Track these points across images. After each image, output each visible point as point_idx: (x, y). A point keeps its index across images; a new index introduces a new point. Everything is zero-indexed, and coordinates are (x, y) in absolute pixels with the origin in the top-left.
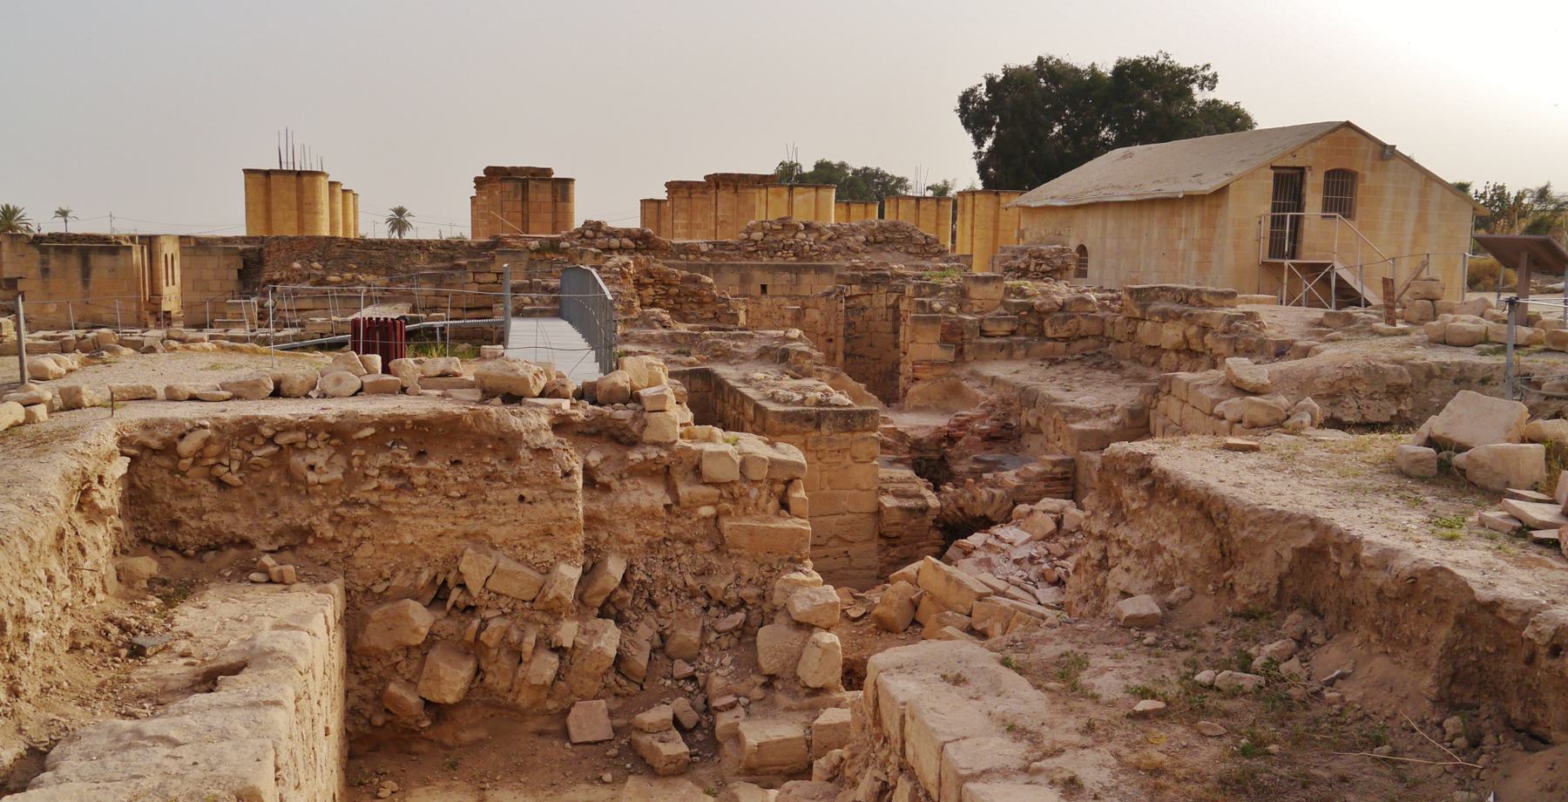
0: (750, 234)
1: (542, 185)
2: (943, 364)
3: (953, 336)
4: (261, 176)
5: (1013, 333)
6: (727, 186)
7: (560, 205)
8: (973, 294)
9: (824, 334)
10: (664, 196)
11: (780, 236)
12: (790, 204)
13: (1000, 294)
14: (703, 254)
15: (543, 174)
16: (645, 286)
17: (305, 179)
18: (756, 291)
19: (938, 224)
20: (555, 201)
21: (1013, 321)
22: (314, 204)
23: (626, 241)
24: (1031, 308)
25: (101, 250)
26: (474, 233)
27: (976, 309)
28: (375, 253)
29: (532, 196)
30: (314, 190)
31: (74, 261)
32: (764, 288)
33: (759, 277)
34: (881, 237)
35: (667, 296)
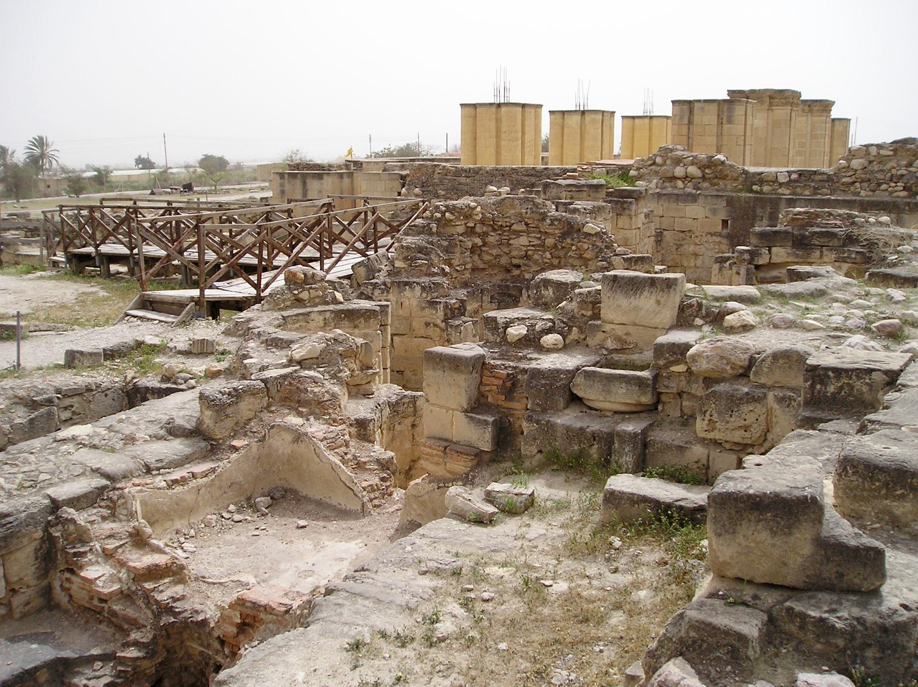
0: (849, 160)
4: (471, 110)
7: (726, 126)
8: (607, 312)
13: (669, 314)
14: (781, 185)
16: (518, 234)
17: (503, 109)
20: (720, 123)
22: (611, 127)
25: (315, 176)
28: (463, 180)
29: (697, 118)
30: (538, 118)
31: (298, 183)
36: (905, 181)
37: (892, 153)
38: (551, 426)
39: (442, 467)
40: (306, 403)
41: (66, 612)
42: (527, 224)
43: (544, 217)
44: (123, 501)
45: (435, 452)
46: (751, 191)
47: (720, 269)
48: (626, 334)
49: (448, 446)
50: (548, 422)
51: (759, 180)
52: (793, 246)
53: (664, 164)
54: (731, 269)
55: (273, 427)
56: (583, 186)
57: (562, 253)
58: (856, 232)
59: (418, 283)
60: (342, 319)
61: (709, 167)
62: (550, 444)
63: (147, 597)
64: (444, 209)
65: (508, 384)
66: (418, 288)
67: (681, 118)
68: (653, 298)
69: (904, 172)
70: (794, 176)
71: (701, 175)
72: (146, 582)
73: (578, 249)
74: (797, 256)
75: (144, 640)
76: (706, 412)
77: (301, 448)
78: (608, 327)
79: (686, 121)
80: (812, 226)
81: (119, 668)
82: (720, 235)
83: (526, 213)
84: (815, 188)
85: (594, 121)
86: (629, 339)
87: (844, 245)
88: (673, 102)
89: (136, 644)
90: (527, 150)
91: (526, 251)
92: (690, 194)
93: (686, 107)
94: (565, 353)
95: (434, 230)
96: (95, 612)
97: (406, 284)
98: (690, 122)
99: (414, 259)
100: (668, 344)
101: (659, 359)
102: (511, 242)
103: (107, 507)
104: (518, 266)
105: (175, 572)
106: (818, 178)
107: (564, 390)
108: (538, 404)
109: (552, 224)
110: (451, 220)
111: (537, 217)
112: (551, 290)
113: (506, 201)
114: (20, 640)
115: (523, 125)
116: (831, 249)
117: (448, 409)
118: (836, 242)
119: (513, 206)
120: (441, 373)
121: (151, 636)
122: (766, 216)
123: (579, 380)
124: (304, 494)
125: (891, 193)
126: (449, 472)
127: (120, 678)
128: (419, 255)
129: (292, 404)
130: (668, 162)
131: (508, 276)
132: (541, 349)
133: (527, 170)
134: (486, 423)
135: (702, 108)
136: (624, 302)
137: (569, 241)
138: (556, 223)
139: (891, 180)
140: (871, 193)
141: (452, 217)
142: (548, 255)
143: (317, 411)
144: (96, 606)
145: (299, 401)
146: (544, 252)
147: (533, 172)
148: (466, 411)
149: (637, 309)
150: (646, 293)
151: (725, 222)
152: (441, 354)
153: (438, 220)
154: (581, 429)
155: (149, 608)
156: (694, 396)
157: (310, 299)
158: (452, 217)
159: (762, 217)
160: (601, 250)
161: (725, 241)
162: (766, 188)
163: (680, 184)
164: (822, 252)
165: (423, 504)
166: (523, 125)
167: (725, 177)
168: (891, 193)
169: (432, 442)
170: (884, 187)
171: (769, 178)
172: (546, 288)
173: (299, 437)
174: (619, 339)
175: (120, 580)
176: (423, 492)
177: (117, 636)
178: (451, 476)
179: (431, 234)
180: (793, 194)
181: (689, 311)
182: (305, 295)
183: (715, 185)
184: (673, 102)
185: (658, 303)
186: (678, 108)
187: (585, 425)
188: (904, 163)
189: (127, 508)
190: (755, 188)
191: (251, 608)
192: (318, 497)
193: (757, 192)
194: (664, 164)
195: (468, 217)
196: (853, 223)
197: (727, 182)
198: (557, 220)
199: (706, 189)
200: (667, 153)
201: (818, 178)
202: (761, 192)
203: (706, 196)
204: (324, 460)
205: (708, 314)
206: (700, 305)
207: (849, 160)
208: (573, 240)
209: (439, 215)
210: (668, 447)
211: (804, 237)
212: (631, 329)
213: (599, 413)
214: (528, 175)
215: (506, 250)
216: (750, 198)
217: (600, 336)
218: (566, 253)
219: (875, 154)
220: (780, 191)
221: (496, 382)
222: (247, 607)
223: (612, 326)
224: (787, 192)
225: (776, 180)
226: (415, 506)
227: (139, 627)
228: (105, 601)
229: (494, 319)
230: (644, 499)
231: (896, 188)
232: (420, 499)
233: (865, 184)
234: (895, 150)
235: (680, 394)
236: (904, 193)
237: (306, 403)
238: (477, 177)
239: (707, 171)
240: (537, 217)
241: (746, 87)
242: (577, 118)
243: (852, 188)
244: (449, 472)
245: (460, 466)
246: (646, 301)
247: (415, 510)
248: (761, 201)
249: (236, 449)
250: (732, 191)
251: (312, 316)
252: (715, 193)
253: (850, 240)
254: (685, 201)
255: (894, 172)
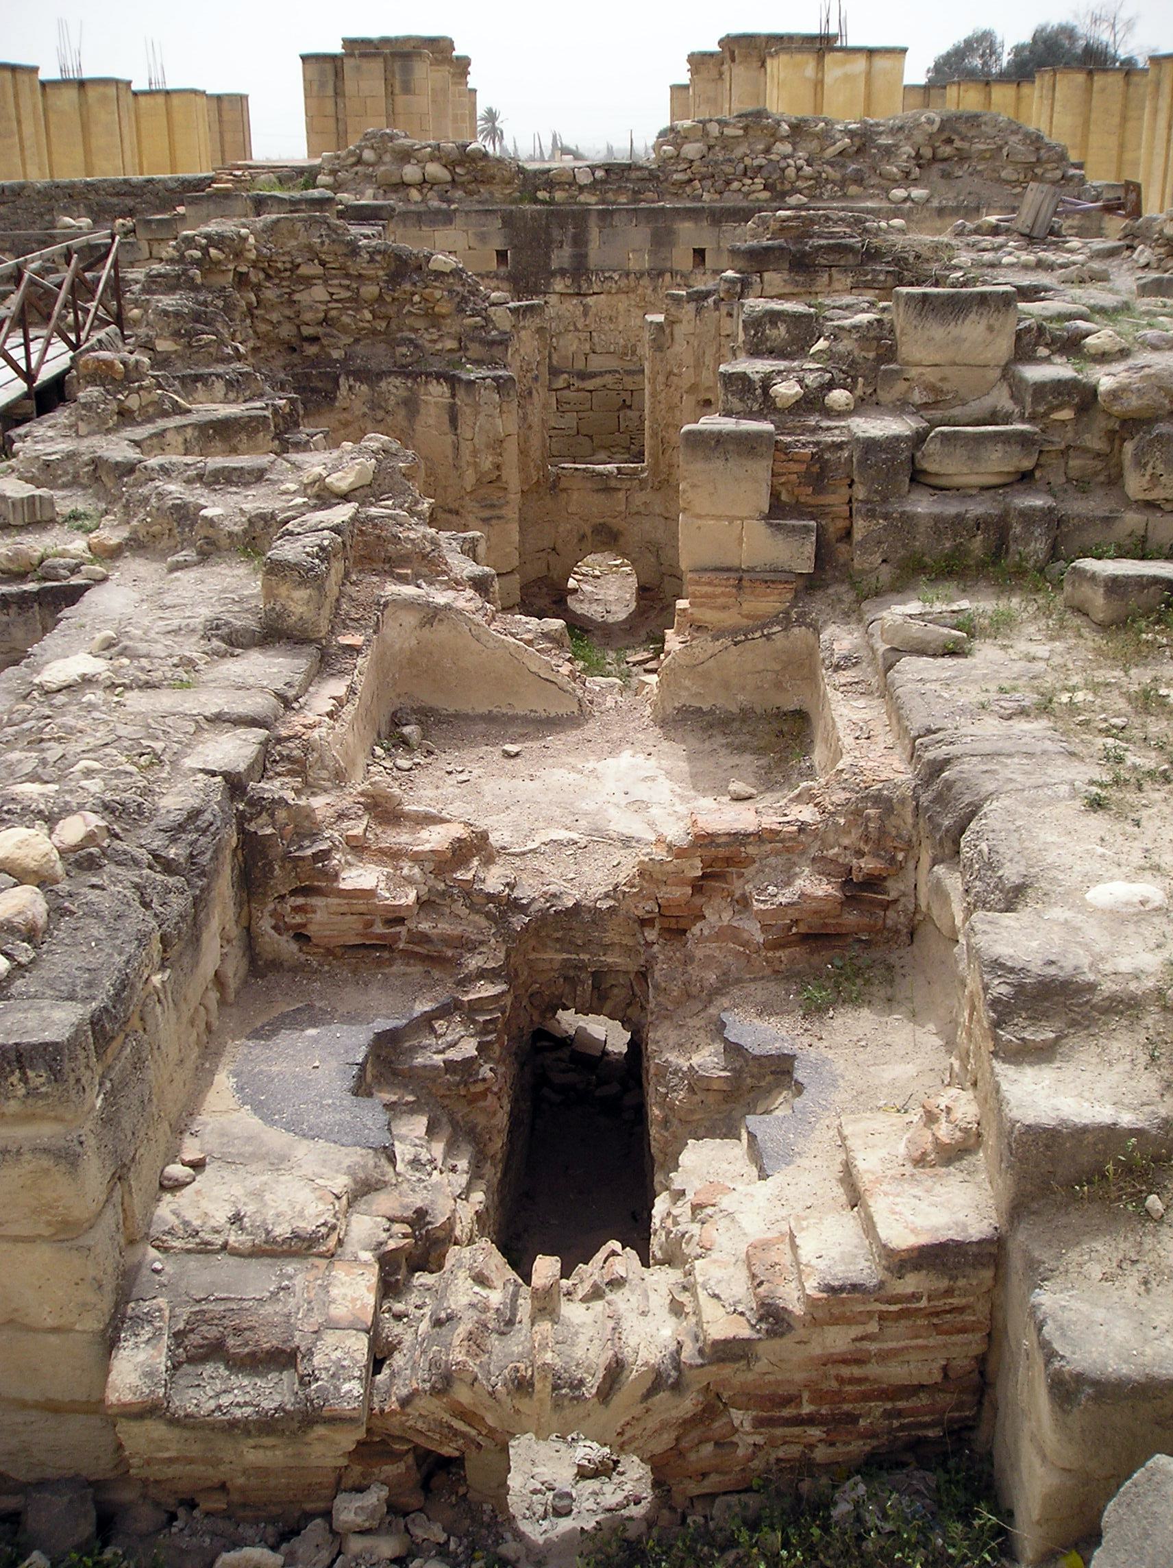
0: (678, 147)
1: (367, 65)
2: (772, 577)
3: (807, 488)
5: (1025, 478)
6: (746, 57)
7: (401, 99)
9: (693, 389)
10: (684, 78)
11: (740, 151)
12: (819, 84)
13: (1003, 347)
14: (582, 188)
15: (439, 48)
16: (308, 281)
18: (682, 259)
19: (1124, 119)
20: (390, 94)
21: (1023, 440)
23: (434, 169)
24: (1085, 398)
26: (312, 153)
27: (917, 397)
29: (350, 86)
32: (700, 254)
33: (689, 234)
34: (947, 150)
35: (356, 301)
36: (765, 174)
37: (741, 132)
38: (908, 519)
39: (734, 610)
40: (404, 560)
41: (298, 968)
42: (323, 264)
43: (353, 250)
44: (316, 755)
45: (719, 590)
46: (536, 201)
47: (698, 311)
48: (943, 379)
49: (741, 578)
50: (903, 513)
51: (546, 183)
52: (790, 270)
53: (379, 161)
54: (717, 309)
55: (386, 605)
56: (299, 201)
57: (392, 310)
58: (876, 242)
59: (218, 376)
60: (210, 439)
61: (461, 163)
62: (904, 546)
63: (468, 892)
64: (204, 241)
65: (816, 469)
66: (219, 386)
67: (322, 85)
68: (984, 322)
69: (764, 162)
70: (600, 174)
71: (449, 178)
72: (454, 871)
73: (424, 299)
74: (796, 284)
75: (492, 965)
76: (1146, 464)
77: (441, 632)
78: (913, 372)
79: (330, 92)
80: (811, 237)
81: (481, 1019)
82: (496, 276)
83: (323, 243)
84: (635, 192)
85: (104, 99)
86: (946, 386)
87: (862, 264)
88: (305, 58)
89: (482, 974)
90: (28, 153)
91: (326, 312)
92: (438, 211)
93: (329, 67)
94: (860, 416)
95: (199, 281)
96: (380, 945)
97: (197, 378)
98: (338, 93)
99: (190, 334)
100: (1052, 381)
101: (1039, 404)
102: (297, 297)
103: (291, 773)
104: (314, 339)
105: (475, 847)
106: (634, 175)
107: (905, 465)
108: (876, 492)
109: (372, 260)
110: (219, 262)
111: (342, 249)
112: (782, 329)
113: (281, 225)
114: (274, 1032)
115: (17, 106)
116: (845, 270)
117: (731, 519)
118: (851, 259)
119: (294, 234)
120: (719, 464)
121: (502, 955)
122: (568, 241)
123: (931, 447)
124: (451, 710)
125: (748, 194)
126: (747, 617)
127: (491, 1032)
128: (199, 326)
129: (375, 566)
130: (387, 158)
131: (295, 358)
132: (828, 412)
133: (114, 184)
134: (807, 529)
135: (358, 68)
136: (938, 332)
137: (407, 287)
138: (378, 258)
139: (745, 174)
140: (717, 196)
141: (222, 256)
142: (368, 315)
143: (425, 571)
144: (382, 936)
145: (388, 560)
146: (357, 310)
147: (126, 188)
148: (768, 517)
149: (958, 341)
150: (972, 316)
151: (501, 255)
152: (720, 432)
153: (197, 263)
154: (958, 515)
155: (478, 912)
156: (1086, 450)
157: (141, 407)
158: (222, 256)
159: (561, 242)
160: (464, 300)
161: (505, 285)
162: (559, 195)
163: (415, 194)
164: (830, 276)
165: (706, 676)
166: (17, 106)
167: (490, 180)
168: (748, 194)
169: (706, 577)
170: (736, 185)
171: (564, 179)
172: (774, 324)
173: (433, 615)
174: (931, 388)
175: (409, 881)
176: (702, 657)
177: (436, 974)
178: (751, 622)
179: (195, 288)
180: (603, 202)
181: (1026, 339)
182: (133, 402)
183: (470, 193)
184: (305, 58)
185: (990, 328)
186: (314, 67)
187: (962, 509)
188: (761, 147)
189: (325, 768)
190: (541, 195)
191: (727, 844)
192: (482, 710)
193: (544, 202)
194: (379, 161)
195: (238, 255)
196: (866, 230)
197: (493, 188)
198: (379, 252)
199: (460, 201)
200: (383, 142)
201: (634, 175)
202: (551, 202)
203: (467, 213)
204: (491, 644)
205: (1054, 340)
206: (1041, 329)
207: (678, 147)
208: (414, 284)
209: (197, 254)
210: (1090, 521)
211: (804, 254)
212: (948, 371)
213: (959, 491)
214: (118, 194)
215: (288, 312)
216: (539, 212)
217: (901, 386)
218: (399, 311)
219: (717, 134)
220: (582, 198)
221: (795, 467)
222: (719, 846)
223: (920, 370)
224: (593, 199)
225: (573, 182)
226: (687, 683)
227: (471, 946)
228: (401, 921)
229: (743, 377)
230: (1156, 580)
231: (753, 187)
232: (700, 669)
233: (708, 183)
234: (746, 128)
235: (1064, 453)
236: (766, 195)
237: (404, 560)
238: (20, 202)
239: (458, 170)
240: (342, 249)
241: (374, 33)
242: (72, 94)
243: (688, 190)
244: (747, 617)
245: (770, 603)
246: (972, 329)
247: (687, 689)
248: (557, 216)
249: (354, 650)
250: (504, 202)
251: (169, 436)
252: (480, 207)
253: (873, 255)
254: (432, 223)
255: (747, 161)
